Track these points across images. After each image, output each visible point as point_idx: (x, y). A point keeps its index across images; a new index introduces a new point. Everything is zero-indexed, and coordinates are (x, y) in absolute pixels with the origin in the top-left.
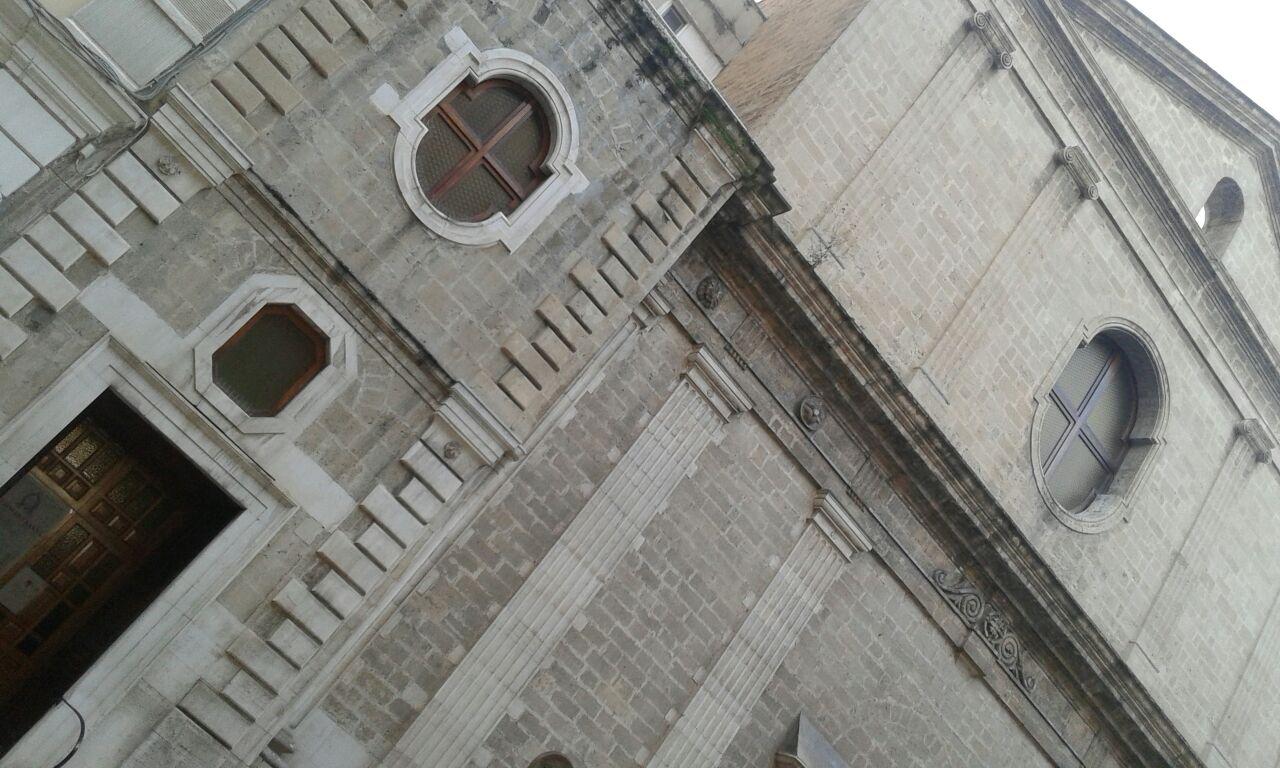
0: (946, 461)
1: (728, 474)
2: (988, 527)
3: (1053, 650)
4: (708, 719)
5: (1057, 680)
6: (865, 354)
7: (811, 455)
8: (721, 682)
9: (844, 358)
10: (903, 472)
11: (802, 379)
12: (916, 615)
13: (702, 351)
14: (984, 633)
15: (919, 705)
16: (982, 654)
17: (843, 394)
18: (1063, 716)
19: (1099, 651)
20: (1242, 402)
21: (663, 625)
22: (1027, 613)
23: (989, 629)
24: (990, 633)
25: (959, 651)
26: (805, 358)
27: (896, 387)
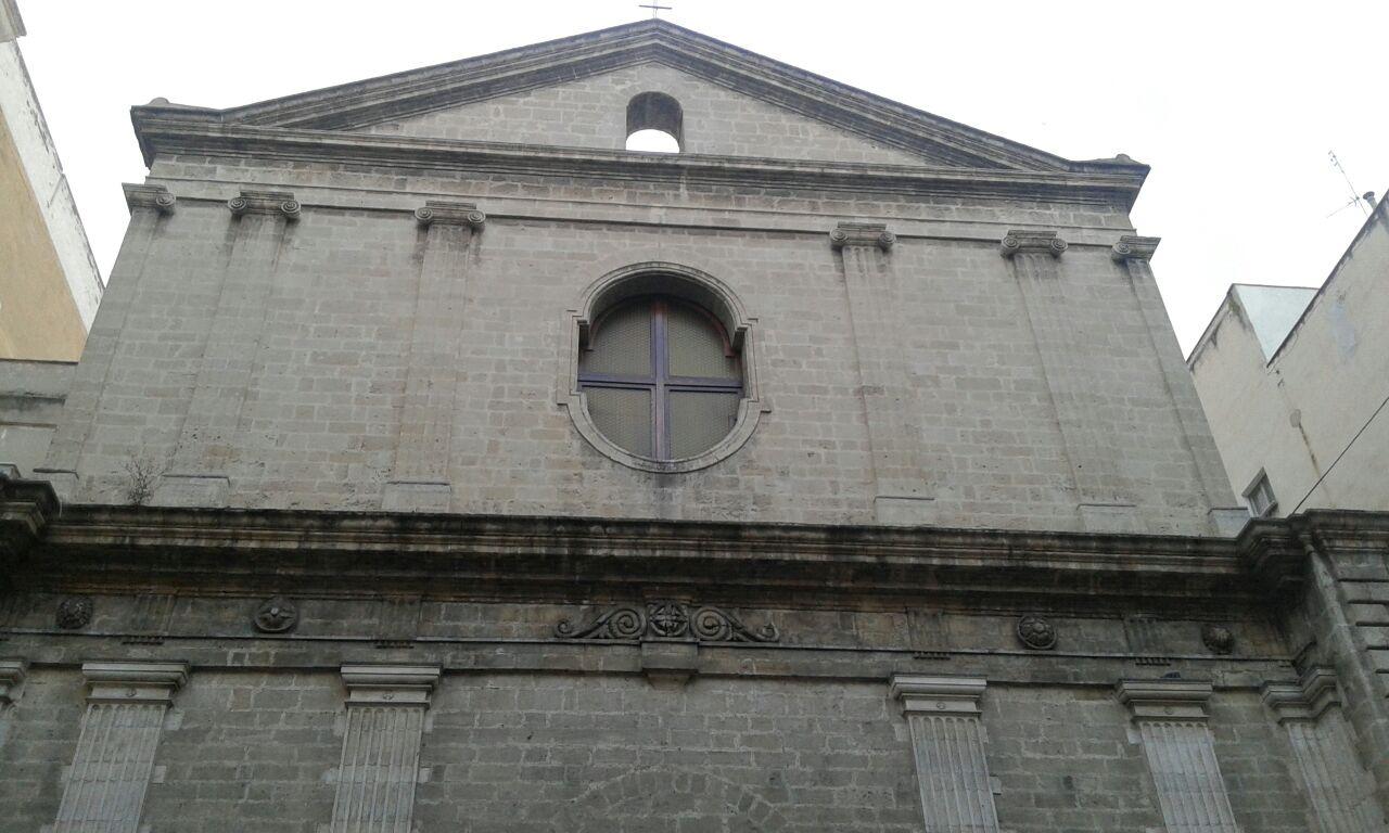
0: (450, 531)
1: (210, 744)
2: (558, 544)
3: (758, 582)
5: (802, 605)
7: (304, 650)
9: (253, 545)
10: (429, 579)
11: (243, 598)
12: (565, 685)
14: (660, 636)
15: (639, 761)
16: (676, 654)
17: (292, 572)
18: (844, 628)
19: (800, 540)
20: (817, 224)
23: (661, 627)
24: (665, 629)
25: (646, 675)
27: (329, 521)
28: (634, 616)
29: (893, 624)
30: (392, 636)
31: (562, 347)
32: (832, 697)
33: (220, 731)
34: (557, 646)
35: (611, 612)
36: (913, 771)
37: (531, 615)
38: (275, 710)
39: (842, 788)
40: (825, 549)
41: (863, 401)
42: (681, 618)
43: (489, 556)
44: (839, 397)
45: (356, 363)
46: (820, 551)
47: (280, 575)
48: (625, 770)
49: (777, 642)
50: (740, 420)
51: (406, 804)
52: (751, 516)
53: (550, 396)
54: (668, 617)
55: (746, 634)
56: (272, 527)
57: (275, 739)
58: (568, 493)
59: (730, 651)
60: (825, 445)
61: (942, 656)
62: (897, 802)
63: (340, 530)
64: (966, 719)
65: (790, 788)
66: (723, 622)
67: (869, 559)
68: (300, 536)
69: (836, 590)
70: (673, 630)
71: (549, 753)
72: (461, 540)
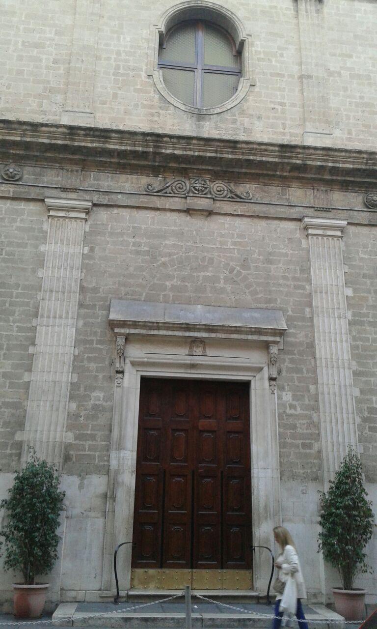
0: (94, 136)
2: (147, 146)
3: (244, 170)
4: (52, 337)
5: (264, 183)
6: (5, 126)
7: (27, 190)
8: (49, 317)
10: (84, 160)
12: (150, 214)
13: (46, 200)
14: (196, 194)
16: (203, 203)
19: (266, 150)
22: (212, 166)
23: (196, 190)
24: (198, 191)
25: (188, 211)
27: (35, 127)
28: (183, 184)
29: (306, 194)
30: (68, 186)
31: (150, 45)
34: (148, 196)
35: (173, 181)
36: (309, 260)
37: (134, 181)
39: (275, 266)
40: (277, 155)
41: (302, 83)
42: (206, 186)
43: (114, 150)
45: (44, 48)
46: (276, 157)
47: (13, 153)
48: (178, 253)
49: (251, 199)
50: (239, 89)
51: (78, 262)
52: (242, 137)
53: (144, 71)
54: (200, 185)
55: (237, 195)
56: (7, 129)
57: (15, 230)
58: (152, 121)
60: (282, 104)
61: (328, 210)
62: (300, 273)
64: (335, 239)
65: (252, 265)
66: (226, 189)
67: (298, 162)
68: (21, 134)
69: (281, 176)
70: (202, 191)
71: (143, 244)
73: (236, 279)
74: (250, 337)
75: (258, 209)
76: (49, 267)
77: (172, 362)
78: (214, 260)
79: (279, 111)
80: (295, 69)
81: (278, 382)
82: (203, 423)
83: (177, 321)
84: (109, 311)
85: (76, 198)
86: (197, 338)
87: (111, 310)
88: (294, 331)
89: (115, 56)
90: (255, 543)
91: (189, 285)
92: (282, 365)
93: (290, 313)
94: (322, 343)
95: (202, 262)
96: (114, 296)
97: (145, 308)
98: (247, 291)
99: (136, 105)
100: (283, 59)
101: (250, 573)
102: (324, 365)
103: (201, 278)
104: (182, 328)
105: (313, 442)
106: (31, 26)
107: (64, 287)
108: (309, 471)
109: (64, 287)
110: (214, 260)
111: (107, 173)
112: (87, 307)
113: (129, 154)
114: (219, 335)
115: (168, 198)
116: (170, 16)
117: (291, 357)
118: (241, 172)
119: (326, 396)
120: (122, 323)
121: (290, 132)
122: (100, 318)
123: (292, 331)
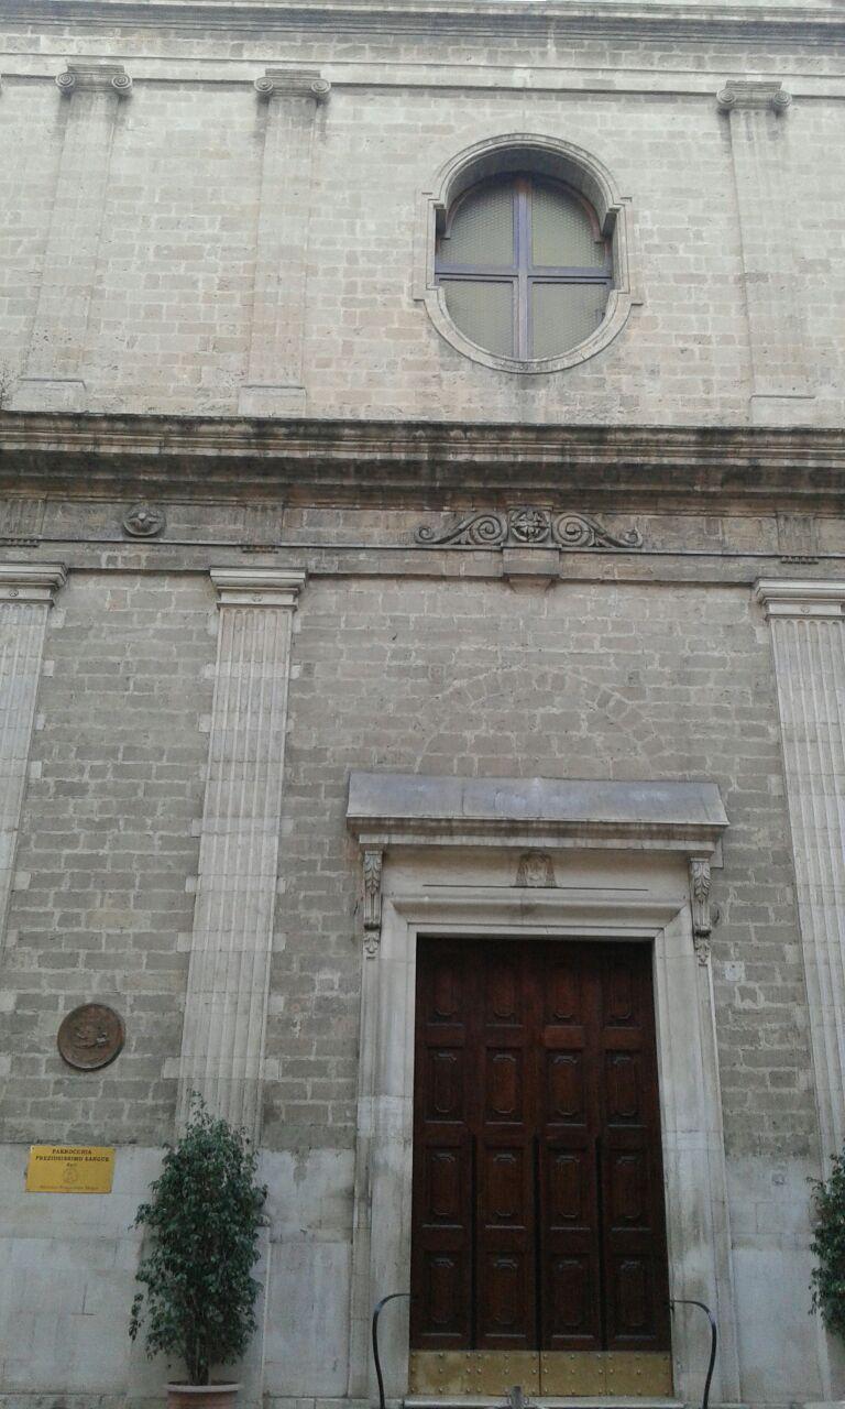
0: (306, 436)
2: (417, 450)
3: (623, 487)
4: (232, 857)
5: (668, 510)
6: (127, 428)
7: (174, 554)
8: (223, 815)
9: (115, 450)
10: (290, 485)
11: (112, 503)
14: (521, 541)
15: (500, 661)
16: (538, 560)
17: (155, 478)
19: (668, 443)
20: (703, 84)
21: (119, 816)
22: (555, 482)
23: (522, 533)
24: (527, 535)
25: (506, 579)
26: (92, 484)
27: (187, 425)
28: (495, 522)
29: (761, 530)
30: (257, 541)
31: (418, 235)
32: (694, 601)
33: (101, 629)
35: (469, 521)
36: (772, 671)
37: (392, 520)
38: (151, 610)
40: (694, 452)
42: (542, 524)
43: (348, 463)
44: (719, 285)
45: (202, 257)
46: (689, 454)
48: (488, 669)
49: (640, 547)
50: (609, 313)
51: (281, 696)
52: (617, 418)
54: (530, 523)
55: (609, 540)
56: (132, 432)
57: (154, 637)
59: (591, 556)
60: (700, 339)
61: (810, 561)
63: (197, 434)
64: (830, 622)
65: (648, 687)
66: (586, 528)
67: (740, 462)
69: (705, 495)
71: (414, 654)
72: (319, 446)
73: (613, 719)
74: (647, 844)
75: (659, 567)
76: (222, 711)
77: (482, 903)
78: (562, 683)
79: (697, 353)
80: (729, 264)
81: (714, 940)
82: (553, 1033)
83: (489, 816)
84: (347, 797)
85: (273, 565)
86: (533, 849)
87: (350, 796)
88: (745, 828)
89: (346, 265)
90: (675, 1294)
91: (512, 736)
92: (722, 904)
93: (735, 788)
94: (808, 851)
95: (539, 686)
96: (356, 765)
97: (420, 789)
98: (640, 744)
99: (392, 364)
100: (700, 243)
101: (666, 1359)
102: (814, 899)
103: (538, 721)
104: (501, 829)
105: (796, 1069)
106: (173, 214)
107: (253, 751)
108: (788, 1135)
109: (253, 751)
110: (562, 683)
111: (336, 508)
112: (302, 791)
113: (379, 467)
114: (581, 843)
115: (464, 554)
116: (455, 173)
117: (739, 884)
118: (616, 492)
119: (822, 967)
120: (373, 822)
121: (721, 398)
122: (328, 813)
123: (741, 826)
